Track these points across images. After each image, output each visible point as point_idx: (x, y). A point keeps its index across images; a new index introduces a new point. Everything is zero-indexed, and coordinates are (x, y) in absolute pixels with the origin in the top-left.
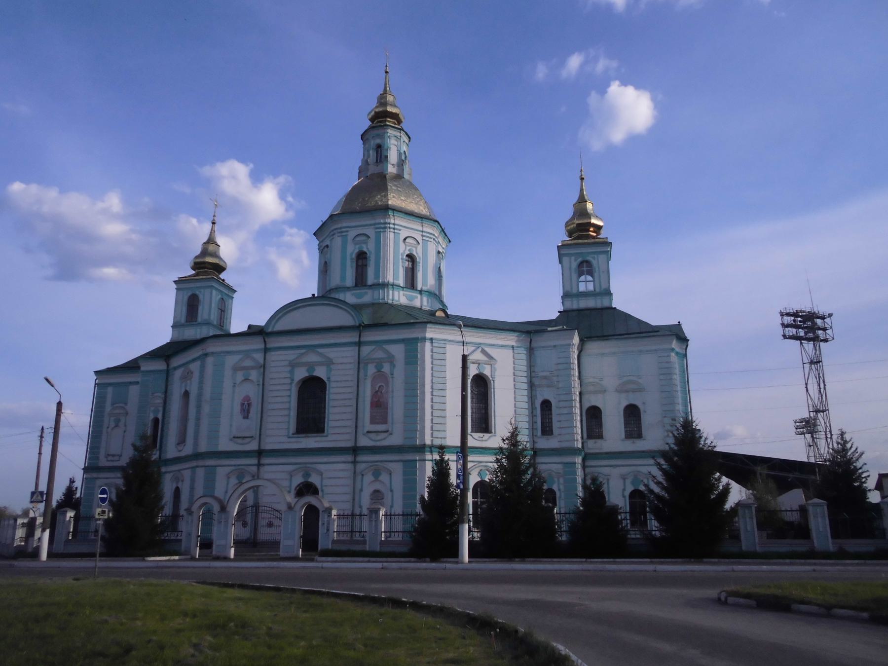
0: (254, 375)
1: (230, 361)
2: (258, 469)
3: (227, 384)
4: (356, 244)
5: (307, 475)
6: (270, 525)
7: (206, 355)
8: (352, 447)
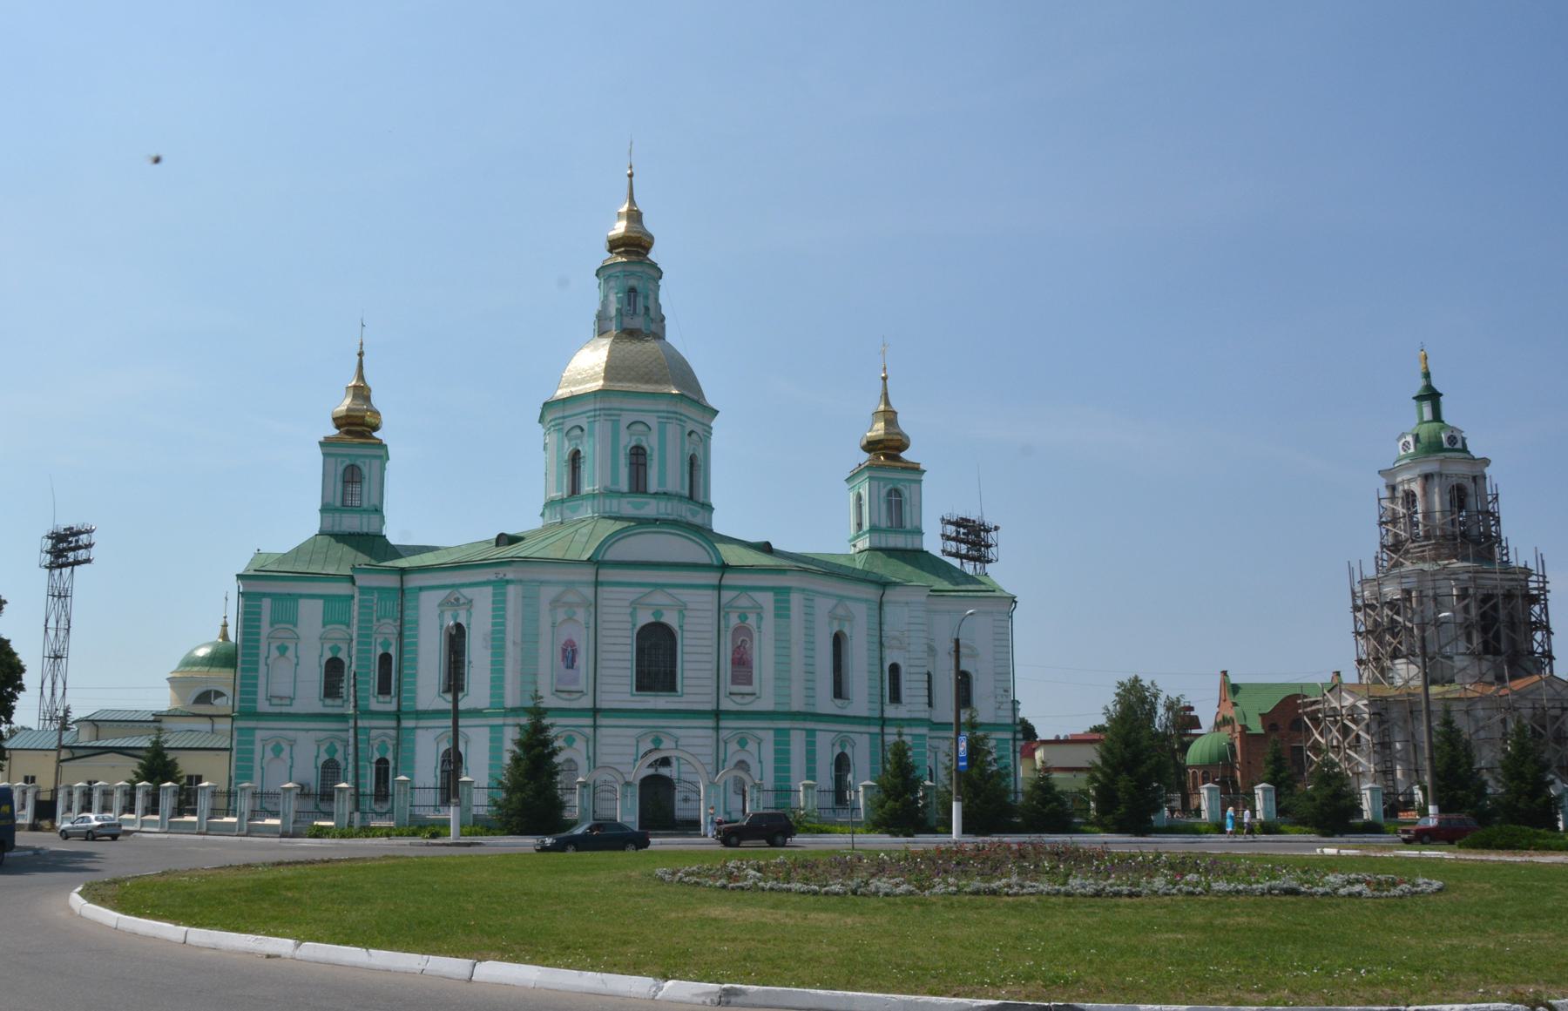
0: (581, 615)
1: (548, 593)
2: (595, 731)
4: (631, 435)
6: (686, 800)
7: (508, 582)
8: (713, 710)
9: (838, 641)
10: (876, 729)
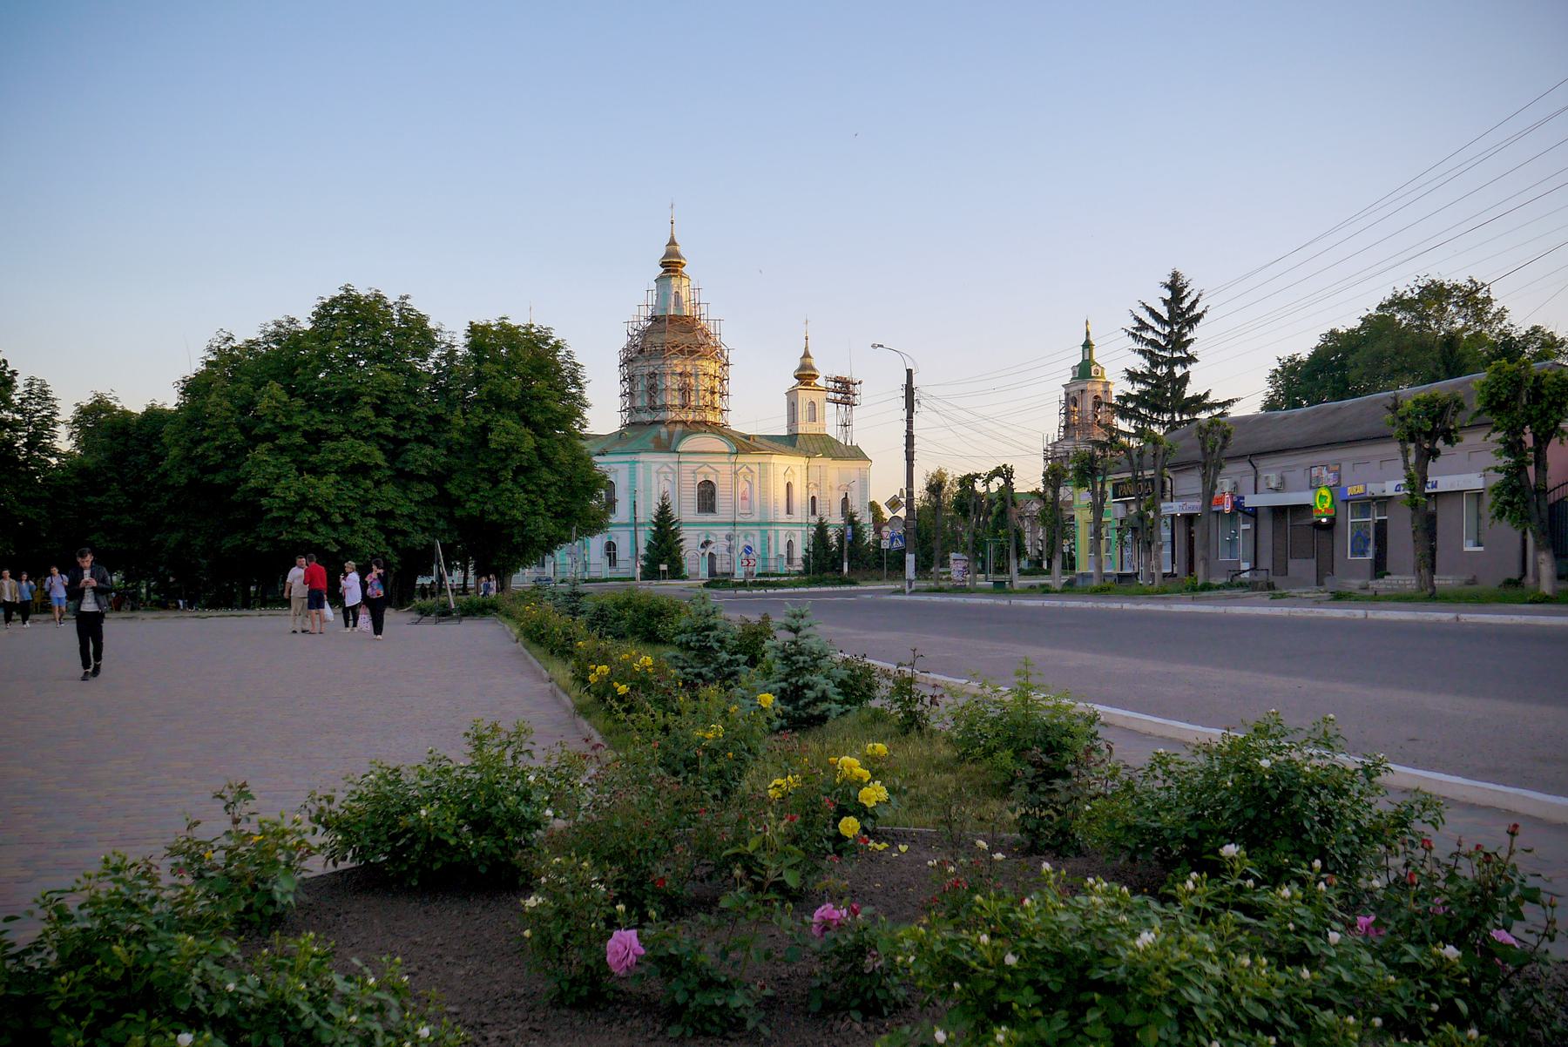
1: (654, 467)
3: (654, 481)
5: (707, 536)
7: (638, 462)
9: (789, 485)
10: (805, 529)
